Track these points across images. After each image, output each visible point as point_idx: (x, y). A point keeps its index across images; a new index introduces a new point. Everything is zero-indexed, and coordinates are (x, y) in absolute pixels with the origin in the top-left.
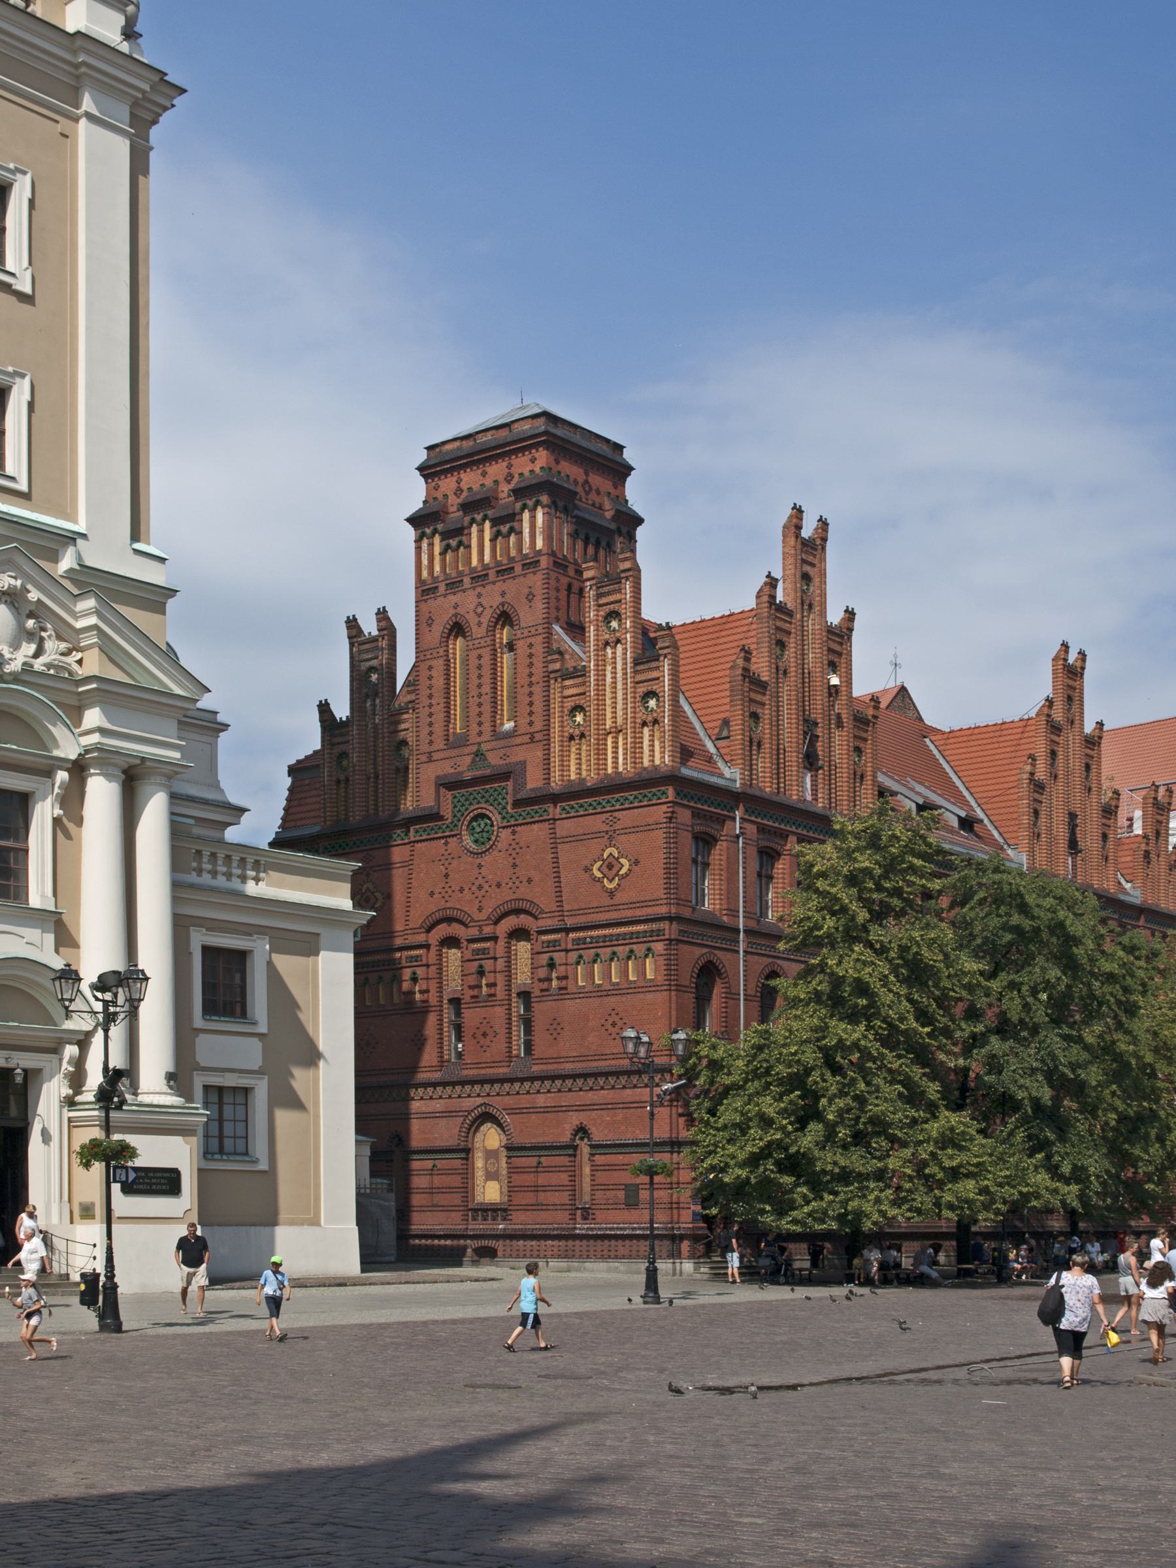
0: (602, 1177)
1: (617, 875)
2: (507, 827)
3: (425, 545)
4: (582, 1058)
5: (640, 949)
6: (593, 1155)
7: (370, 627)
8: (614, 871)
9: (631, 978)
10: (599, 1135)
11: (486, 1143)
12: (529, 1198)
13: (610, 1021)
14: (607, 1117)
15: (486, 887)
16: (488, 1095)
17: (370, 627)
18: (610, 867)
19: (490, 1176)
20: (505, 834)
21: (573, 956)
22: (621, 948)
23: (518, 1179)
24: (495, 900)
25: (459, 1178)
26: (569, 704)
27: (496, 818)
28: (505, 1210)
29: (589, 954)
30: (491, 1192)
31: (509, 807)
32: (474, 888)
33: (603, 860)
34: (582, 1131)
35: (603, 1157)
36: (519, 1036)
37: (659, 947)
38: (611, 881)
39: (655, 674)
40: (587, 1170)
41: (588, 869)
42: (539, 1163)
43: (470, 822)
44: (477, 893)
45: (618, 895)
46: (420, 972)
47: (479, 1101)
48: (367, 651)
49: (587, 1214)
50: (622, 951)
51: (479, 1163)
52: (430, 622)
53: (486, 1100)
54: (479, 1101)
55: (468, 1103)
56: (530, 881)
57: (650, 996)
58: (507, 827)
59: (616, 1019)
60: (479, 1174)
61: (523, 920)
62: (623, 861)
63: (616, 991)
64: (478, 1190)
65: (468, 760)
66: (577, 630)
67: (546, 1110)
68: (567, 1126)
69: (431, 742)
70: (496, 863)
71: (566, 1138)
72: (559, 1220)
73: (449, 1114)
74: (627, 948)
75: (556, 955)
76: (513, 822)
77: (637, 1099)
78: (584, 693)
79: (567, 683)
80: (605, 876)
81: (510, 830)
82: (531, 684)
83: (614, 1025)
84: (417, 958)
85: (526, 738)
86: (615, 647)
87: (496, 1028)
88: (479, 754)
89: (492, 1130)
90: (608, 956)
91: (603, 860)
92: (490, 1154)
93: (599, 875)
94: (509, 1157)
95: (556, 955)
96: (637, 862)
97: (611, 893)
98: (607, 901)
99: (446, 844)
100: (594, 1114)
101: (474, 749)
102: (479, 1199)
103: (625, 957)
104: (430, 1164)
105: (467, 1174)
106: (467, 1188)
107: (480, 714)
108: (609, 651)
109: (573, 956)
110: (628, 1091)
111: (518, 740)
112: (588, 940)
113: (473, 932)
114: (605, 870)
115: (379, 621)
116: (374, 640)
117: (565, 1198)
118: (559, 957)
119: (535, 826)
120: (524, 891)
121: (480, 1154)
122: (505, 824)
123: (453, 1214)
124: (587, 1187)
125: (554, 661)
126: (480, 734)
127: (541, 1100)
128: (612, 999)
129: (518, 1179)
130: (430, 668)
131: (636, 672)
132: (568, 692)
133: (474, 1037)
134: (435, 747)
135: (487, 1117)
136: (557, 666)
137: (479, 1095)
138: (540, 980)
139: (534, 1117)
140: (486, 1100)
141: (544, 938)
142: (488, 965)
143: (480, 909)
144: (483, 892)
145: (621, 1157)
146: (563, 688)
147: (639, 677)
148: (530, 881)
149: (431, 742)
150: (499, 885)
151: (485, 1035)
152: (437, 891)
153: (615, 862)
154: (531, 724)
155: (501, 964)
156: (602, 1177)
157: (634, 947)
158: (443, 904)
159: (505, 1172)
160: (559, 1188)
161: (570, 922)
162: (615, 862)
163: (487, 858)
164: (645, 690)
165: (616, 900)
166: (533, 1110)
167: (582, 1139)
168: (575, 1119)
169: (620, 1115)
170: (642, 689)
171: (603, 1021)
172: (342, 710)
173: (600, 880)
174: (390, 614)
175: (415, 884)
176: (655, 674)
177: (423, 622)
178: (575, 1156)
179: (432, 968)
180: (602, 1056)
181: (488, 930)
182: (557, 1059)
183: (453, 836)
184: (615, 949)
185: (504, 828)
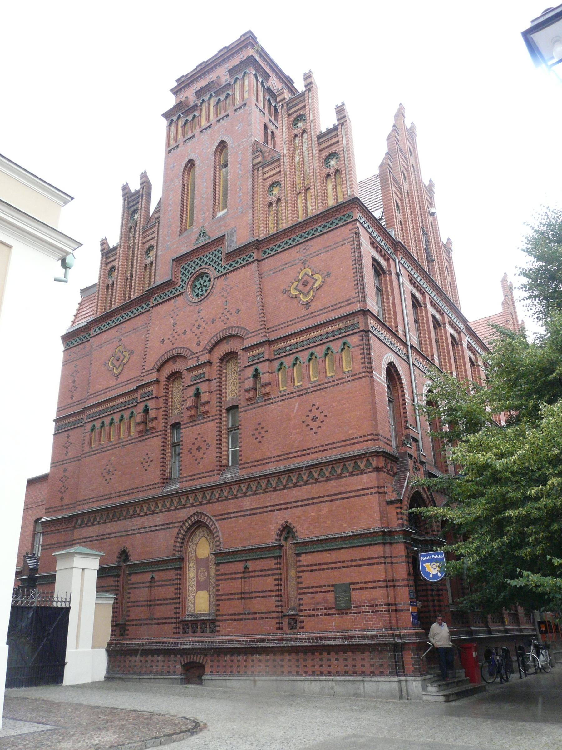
0: (309, 579)
1: (311, 289)
2: (220, 276)
3: (173, 129)
4: (287, 456)
5: (336, 346)
6: (298, 555)
7: (135, 186)
8: (309, 287)
9: (329, 374)
10: (303, 533)
11: (198, 551)
12: (236, 606)
13: (311, 417)
14: (312, 512)
15: (204, 325)
16: (201, 504)
18: (305, 284)
19: (200, 586)
20: (219, 282)
21: (276, 364)
22: (318, 348)
23: (226, 587)
24: (211, 333)
25: (172, 589)
26: (269, 182)
27: (212, 273)
28: (213, 621)
29: (288, 361)
30: (200, 603)
32: (195, 329)
33: (299, 280)
34: (287, 530)
35: (309, 557)
36: (228, 447)
37: (354, 340)
38: (306, 295)
39: (334, 140)
40: (292, 573)
41: (285, 291)
42: (246, 568)
43: (193, 282)
44: (197, 332)
45: (313, 304)
46: (151, 404)
47: (193, 510)
48: (133, 201)
49: (294, 622)
50: (319, 351)
51: (191, 573)
53: (198, 509)
54: (193, 510)
55: (183, 514)
56: (238, 311)
57: (348, 386)
58: (220, 276)
59: (317, 413)
60: (191, 584)
61: (233, 346)
62: (315, 276)
63: (317, 388)
64: (190, 600)
67: (253, 512)
68: (272, 527)
70: (213, 306)
71: (271, 541)
72: (267, 632)
73: (168, 525)
74: (324, 347)
75: (259, 367)
76: (225, 272)
77: (342, 489)
78: (280, 172)
80: (301, 292)
83: (315, 419)
84: (150, 392)
86: (302, 136)
87: (209, 442)
89: (203, 539)
90: (307, 358)
91: (299, 280)
92: (201, 563)
93: (294, 293)
94: (218, 564)
95: (259, 367)
96: (328, 274)
97: (307, 305)
98: (304, 312)
99: (175, 302)
100: (298, 511)
102: (189, 610)
103: (322, 355)
104: (148, 577)
105: (180, 584)
106: (179, 600)
108: (297, 141)
109: (276, 364)
110: (333, 483)
112: (288, 348)
113: (192, 363)
114: (301, 287)
115: (141, 178)
117: (271, 604)
119: (242, 270)
120: (234, 321)
121: (192, 564)
122: (219, 274)
123: (166, 627)
124: (292, 592)
125: (257, 157)
127: (248, 503)
128: (312, 396)
129: (226, 587)
131: (319, 144)
132: (266, 176)
133: (190, 452)
135: (198, 525)
136: (260, 159)
137: (192, 505)
138: (247, 391)
139: (240, 520)
140: (198, 509)
141: (250, 354)
142: (203, 388)
143: (198, 345)
144: (201, 329)
145: (328, 555)
146: (264, 173)
147: (322, 146)
148: (238, 311)
150: (213, 321)
151: (199, 449)
152: (166, 339)
153: (309, 279)
155: (214, 384)
156: (309, 579)
157: (330, 345)
158: (171, 347)
159: (213, 581)
160: (265, 594)
161: (272, 337)
162: (309, 279)
163: (205, 303)
164: (327, 154)
165: (313, 308)
166: (240, 513)
167: (286, 539)
168: (279, 518)
169: (325, 508)
170: (325, 153)
171: (304, 418)
172: (114, 241)
174: (148, 174)
175: (151, 337)
176: (334, 140)
178: (280, 557)
179: (161, 399)
180: (305, 452)
181: (204, 359)
182: (262, 462)
183: (180, 295)
184: (313, 350)
185: (218, 278)
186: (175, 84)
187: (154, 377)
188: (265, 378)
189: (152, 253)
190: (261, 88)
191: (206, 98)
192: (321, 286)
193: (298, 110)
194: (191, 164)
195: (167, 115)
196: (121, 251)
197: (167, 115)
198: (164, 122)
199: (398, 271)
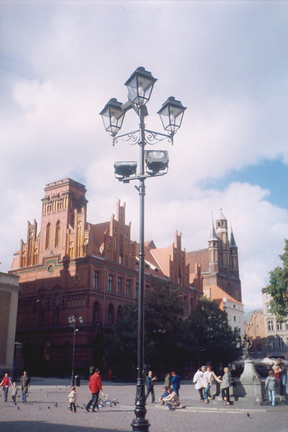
7: (32, 223)
17: (32, 223)
31: (57, 264)
38: (77, 281)
52: (44, 222)
62: (80, 277)
65: (50, 253)
66: (73, 225)
69: (42, 249)
78: (73, 239)
79: (71, 236)
80: (76, 280)
81: (57, 269)
82: (63, 236)
85: (61, 248)
88: (52, 252)
97: (77, 284)
99: (44, 272)
101: (51, 250)
107: (52, 243)
111: (60, 249)
116: (33, 226)
118: (65, 300)
126: (52, 247)
130: (43, 232)
134: (43, 250)
149: (42, 249)
154: (62, 245)
172: (25, 241)
173: (75, 281)
177: (43, 222)
186: (45, 187)
187: (36, 295)
188: (65, 303)
189: (37, 251)
190: (72, 201)
191: (55, 200)
192: (80, 280)
193: (80, 219)
194: (49, 224)
195: (42, 200)
196: (27, 246)
197: (42, 200)
198: (42, 203)
199: (104, 270)
